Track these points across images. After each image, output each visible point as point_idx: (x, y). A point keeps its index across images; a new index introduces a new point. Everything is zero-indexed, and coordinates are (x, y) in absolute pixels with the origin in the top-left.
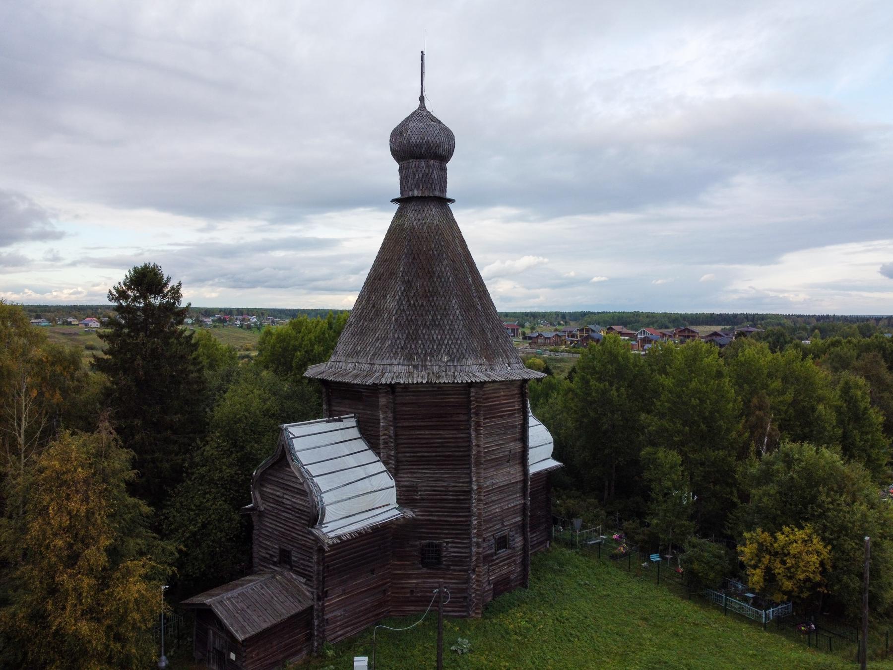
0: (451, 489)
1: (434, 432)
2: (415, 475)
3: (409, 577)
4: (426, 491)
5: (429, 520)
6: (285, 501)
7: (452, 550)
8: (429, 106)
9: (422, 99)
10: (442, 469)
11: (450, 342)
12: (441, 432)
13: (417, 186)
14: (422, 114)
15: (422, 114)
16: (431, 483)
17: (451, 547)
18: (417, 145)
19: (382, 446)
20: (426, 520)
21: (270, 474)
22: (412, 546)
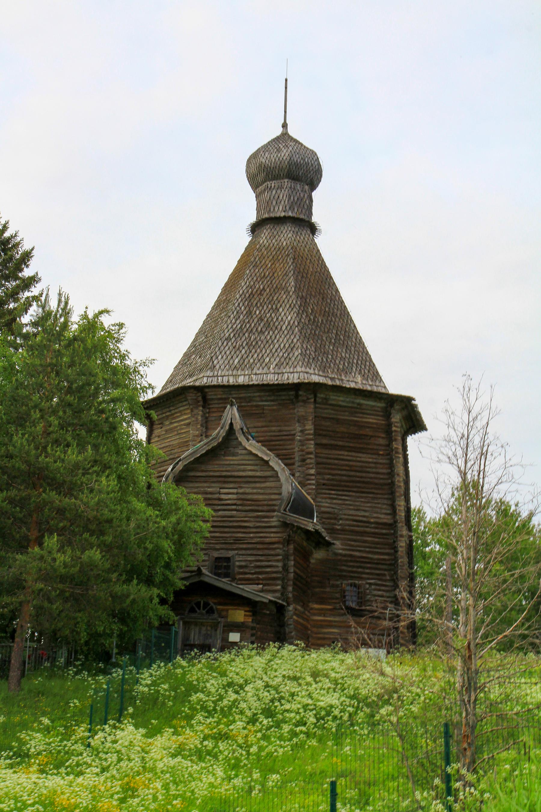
0: (372, 520)
1: (353, 454)
2: (335, 501)
3: (330, 625)
4: (347, 520)
5: (351, 556)
6: (223, 497)
7: (376, 592)
8: (291, 132)
9: (285, 125)
10: (362, 497)
11: (360, 362)
12: (360, 455)
13: (291, 208)
14: (285, 137)
15: (285, 137)
16: (352, 512)
17: (375, 590)
18: (297, 165)
19: (297, 464)
20: (345, 555)
21: (193, 470)
22: (333, 586)
